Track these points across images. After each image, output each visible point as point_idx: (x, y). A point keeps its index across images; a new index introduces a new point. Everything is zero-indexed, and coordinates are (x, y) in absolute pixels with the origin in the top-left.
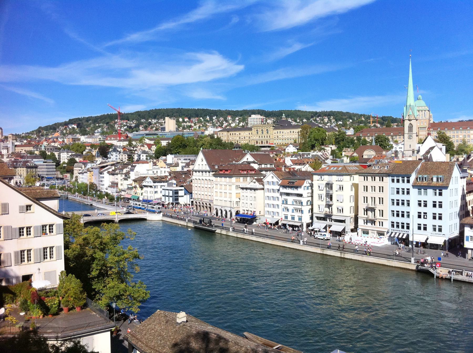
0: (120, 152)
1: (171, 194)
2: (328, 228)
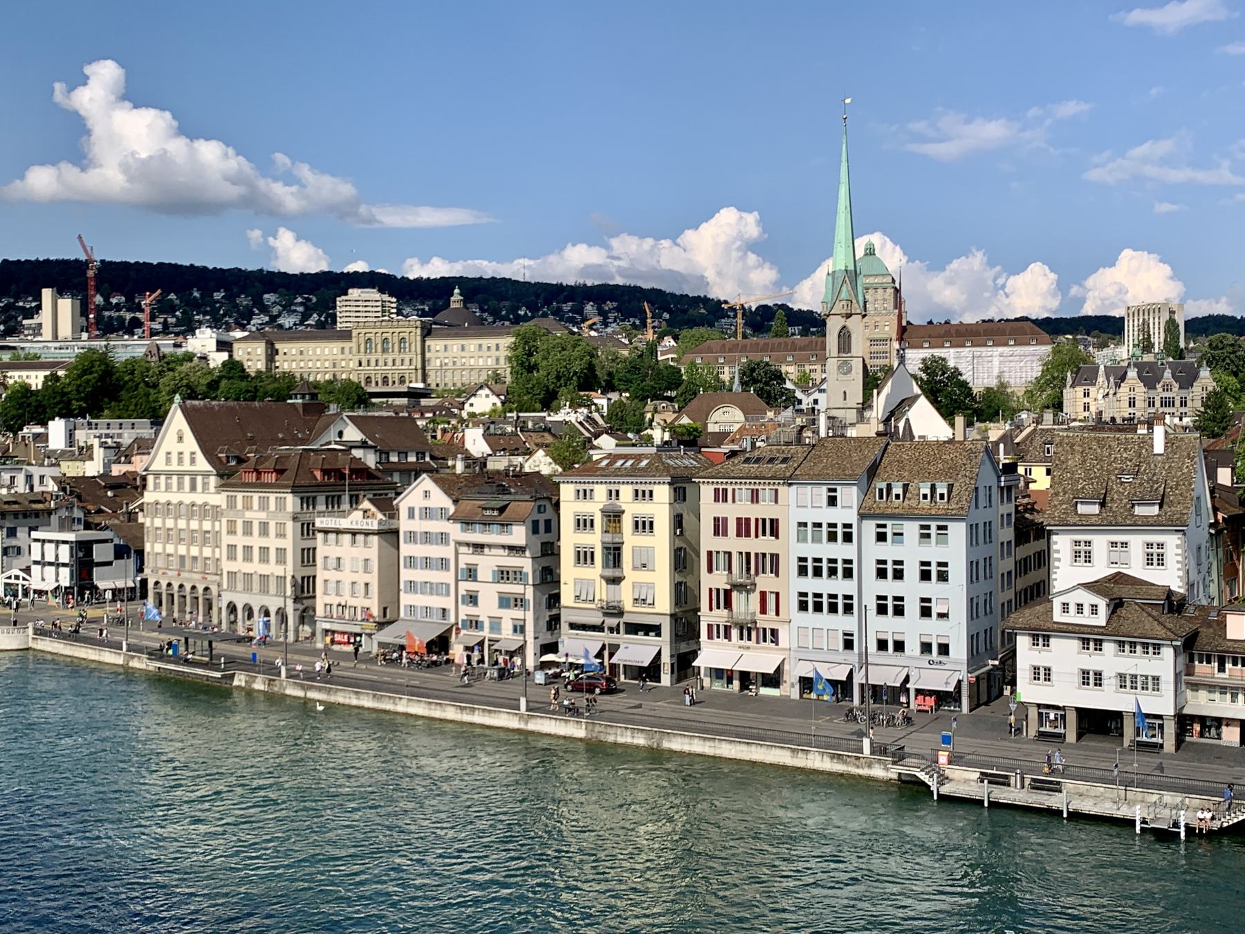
2: (606, 653)
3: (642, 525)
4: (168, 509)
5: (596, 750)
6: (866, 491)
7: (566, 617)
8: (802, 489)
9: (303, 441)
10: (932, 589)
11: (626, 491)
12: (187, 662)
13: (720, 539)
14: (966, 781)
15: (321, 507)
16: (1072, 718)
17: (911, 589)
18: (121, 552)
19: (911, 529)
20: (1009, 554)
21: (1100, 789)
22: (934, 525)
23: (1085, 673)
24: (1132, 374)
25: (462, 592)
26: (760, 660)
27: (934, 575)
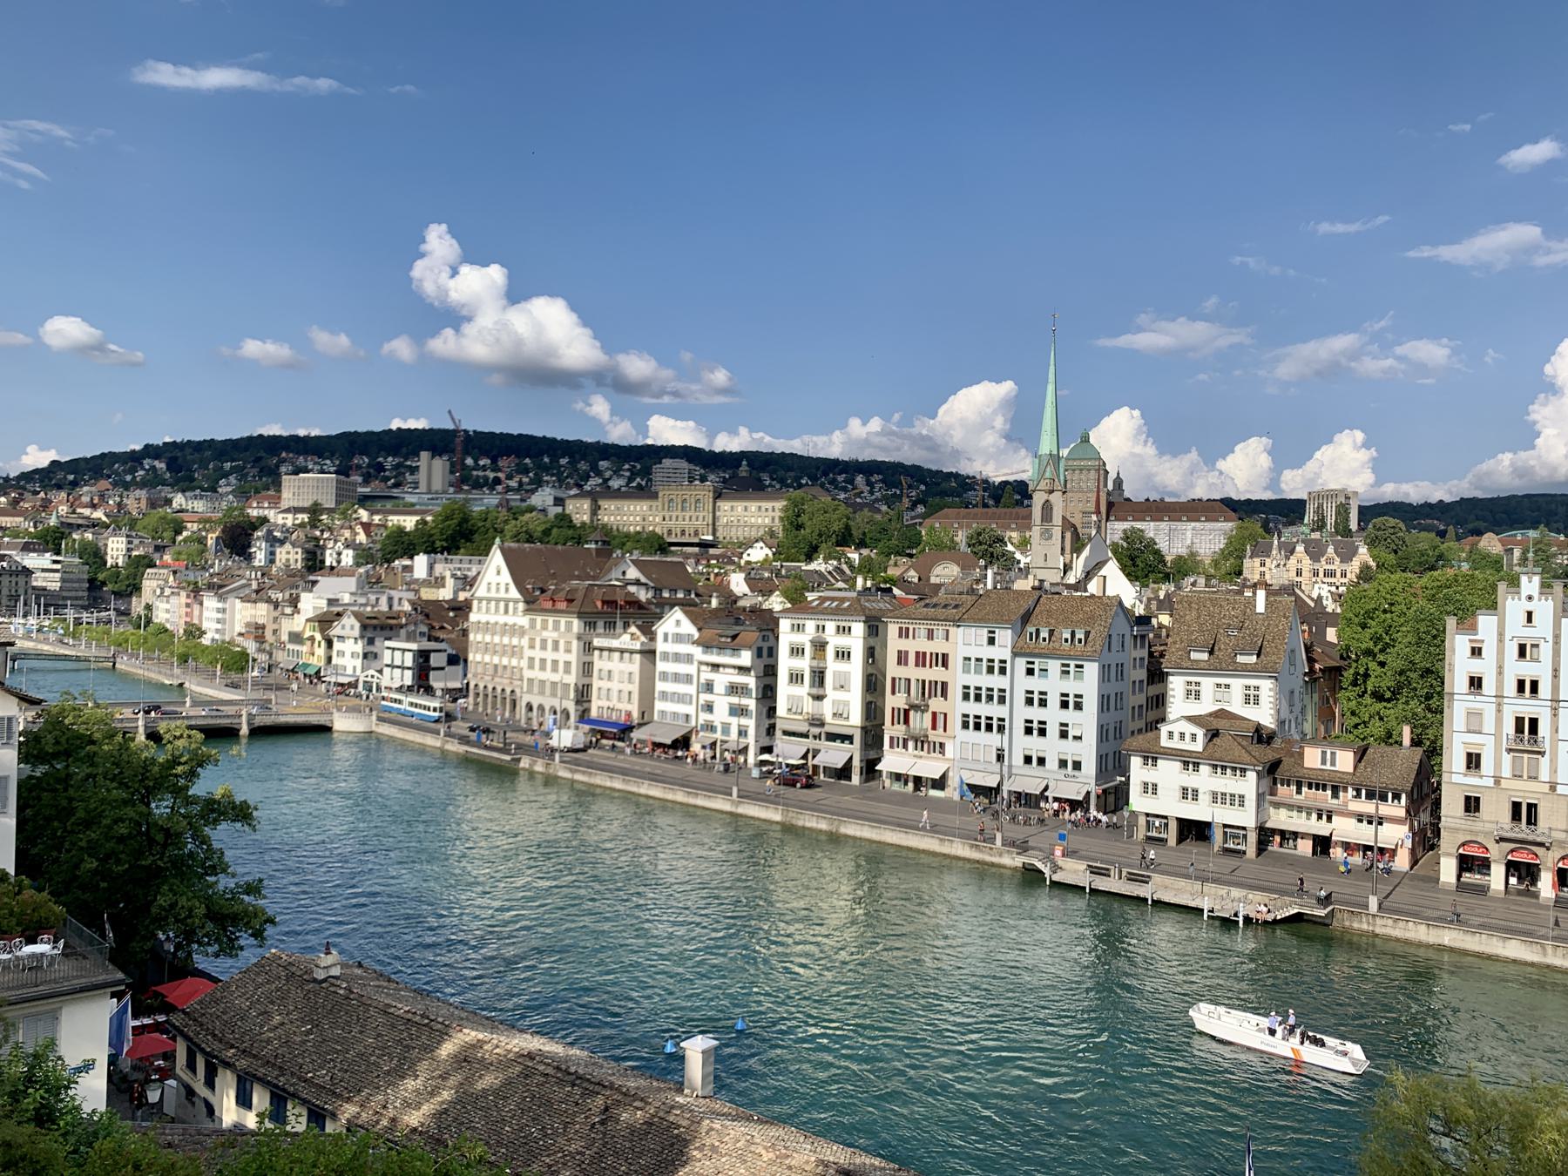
1: (409, 662)
3: (843, 655)
4: (486, 627)
5: (788, 829)
6: (1019, 634)
7: (780, 725)
8: (968, 630)
9: (594, 578)
10: (1070, 716)
11: (831, 627)
12: (486, 748)
13: (902, 668)
14: (1076, 872)
15: (600, 630)
16: (1173, 826)
17: (1053, 715)
18: (453, 660)
19: (1054, 666)
20: (1141, 690)
21: (1181, 883)
22: (1072, 664)
23: (1185, 790)
24: (1300, 548)
25: (701, 702)
26: (929, 767)
27: (1071, 705)
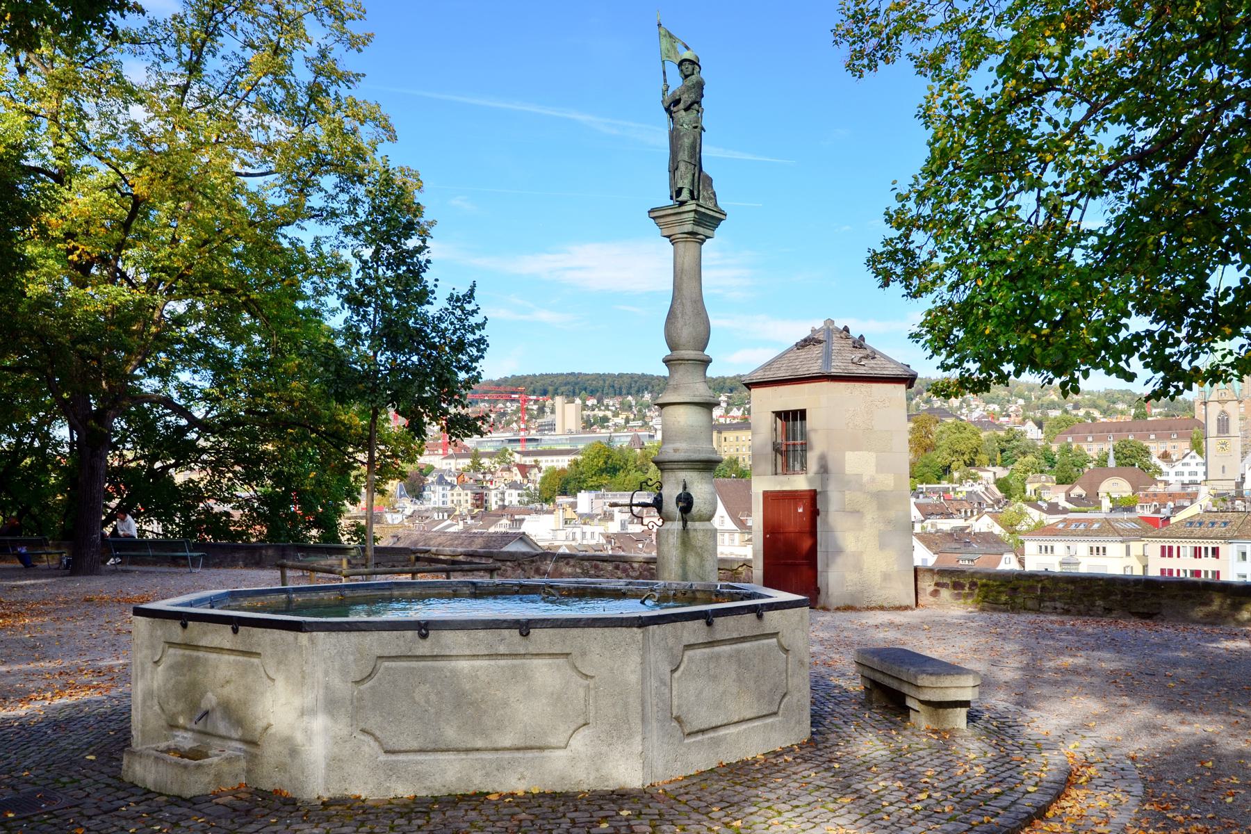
0: (453, 486)
